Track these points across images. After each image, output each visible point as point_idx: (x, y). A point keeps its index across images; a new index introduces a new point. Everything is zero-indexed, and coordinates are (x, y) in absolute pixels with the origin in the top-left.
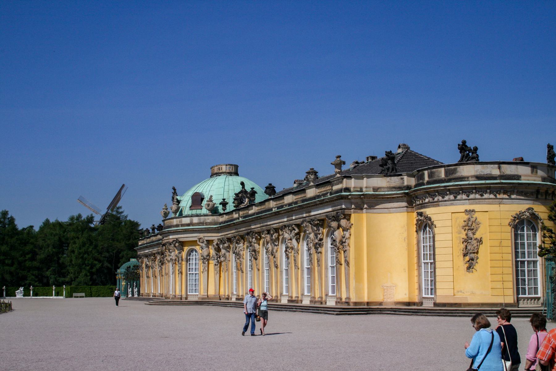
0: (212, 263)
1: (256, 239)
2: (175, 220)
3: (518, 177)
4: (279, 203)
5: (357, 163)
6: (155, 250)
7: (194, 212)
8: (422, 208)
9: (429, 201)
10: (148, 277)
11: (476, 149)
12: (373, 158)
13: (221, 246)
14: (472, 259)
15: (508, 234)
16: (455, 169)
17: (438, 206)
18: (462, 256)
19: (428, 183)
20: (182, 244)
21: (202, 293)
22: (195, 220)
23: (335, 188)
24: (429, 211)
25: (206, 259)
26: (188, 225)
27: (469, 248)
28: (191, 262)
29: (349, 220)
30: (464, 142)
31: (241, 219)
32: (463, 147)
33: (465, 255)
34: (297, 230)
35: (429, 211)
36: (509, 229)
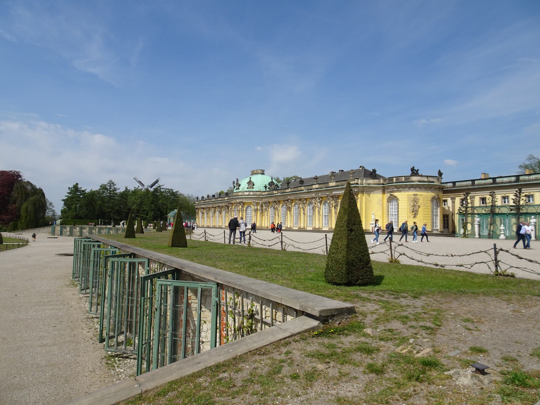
3: (433, 182)
4: (310, 187)
7: (249, 190)
10: (203, 217)
11: (418, 170)
12: (342, 171)
15: (429, 204)
19: (396, 183)
20: (244, 203)
22: (251, 193)
24: (395, 194)
25: (256, 210)
30: (414, 167)
31: (279, 194)
32: (413, 169)
35: (395, 194)
36: (430, 202)
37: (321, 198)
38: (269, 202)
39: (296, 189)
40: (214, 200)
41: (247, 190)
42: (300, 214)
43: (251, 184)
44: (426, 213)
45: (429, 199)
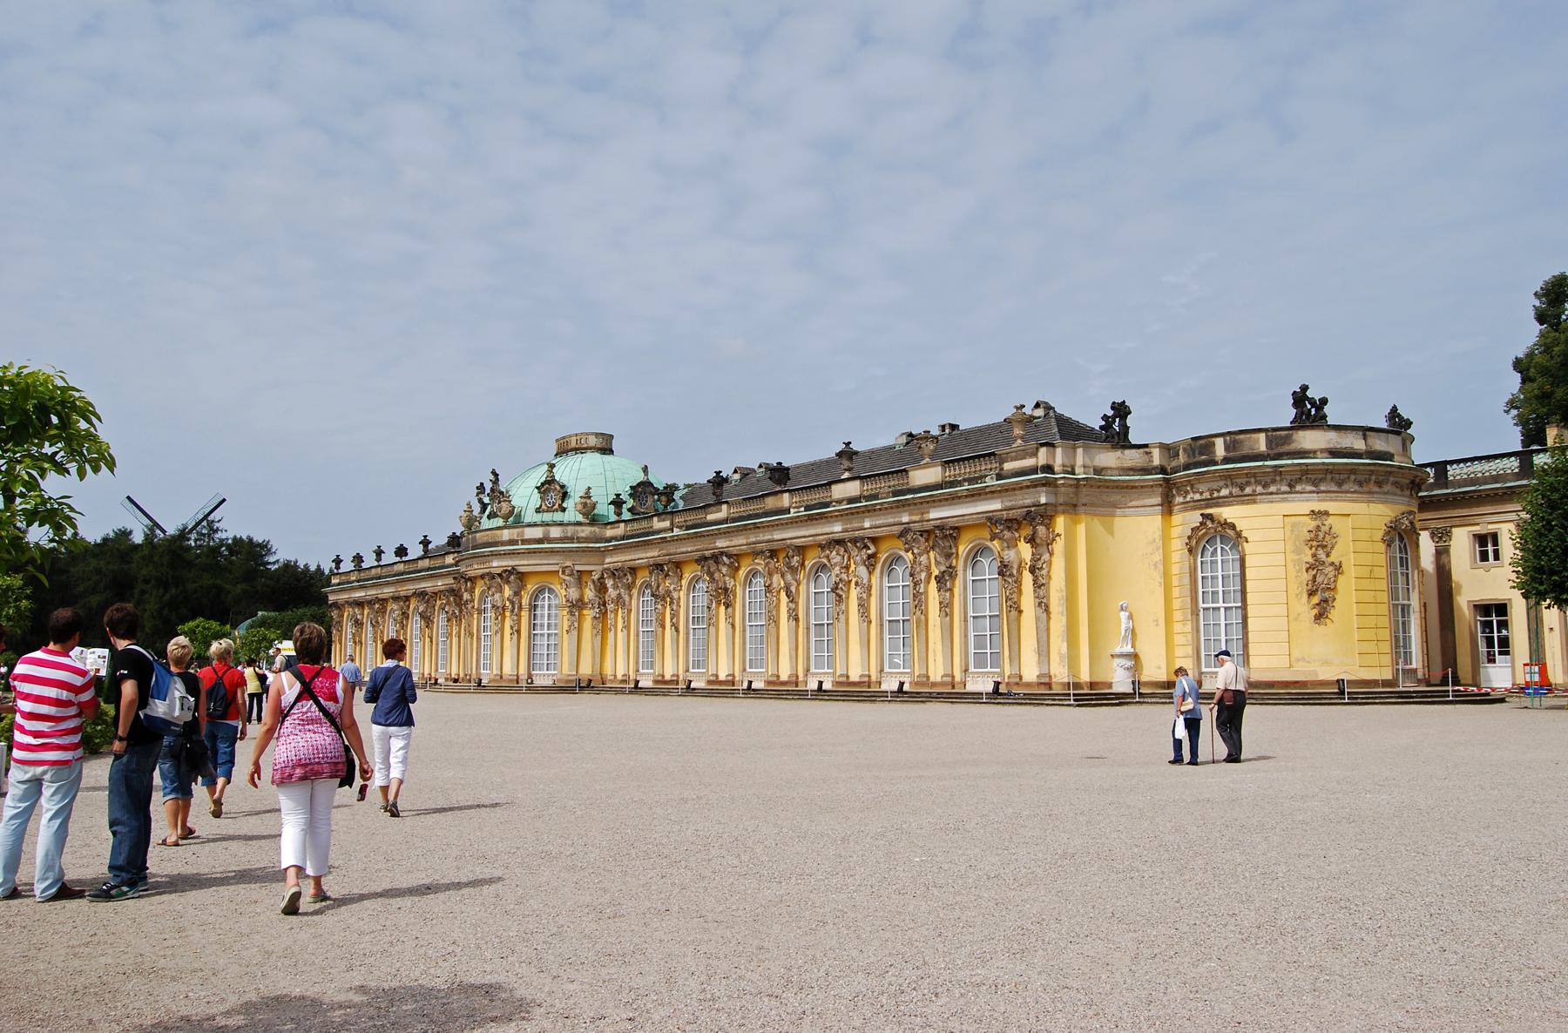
0: (589, 614)
1: (730, 566)
2: (506, 532)
3: (1390, 456)
4: (816, 497)
5: (910, 435)
6: (388, 591)
7: (547, 517)
8: (1208, 506)
9: (1231, 495)
11: (1324, 401)
12: (954, 427)
13: (609, 583)
14: (1326, 601)
16: (1289, 437)
17: (1255, 502)
18: (1305, 596)
19: (1226, 460)
20: (522, 577)
21: (566, 671)
22: (555, 532)
23: (1008, 466)
24: (1227, 513)
26: (539, 541)
27: (1319, 579)
28: (538, 612)
29: (1048, 527)
30: (1305, 388)
31: (677, 532)
32: (1300, 398)
33: (1311, 594)
34: (872, 550)
36: (1382, 547)
37: (874, 540)
38: (634, 570)
39: (752, 508)
40: (401, 567)
41: (538, 518)
42: (774, 620)
43: (552, 489)
44: (1369, 596)
45: (1379, 534)
